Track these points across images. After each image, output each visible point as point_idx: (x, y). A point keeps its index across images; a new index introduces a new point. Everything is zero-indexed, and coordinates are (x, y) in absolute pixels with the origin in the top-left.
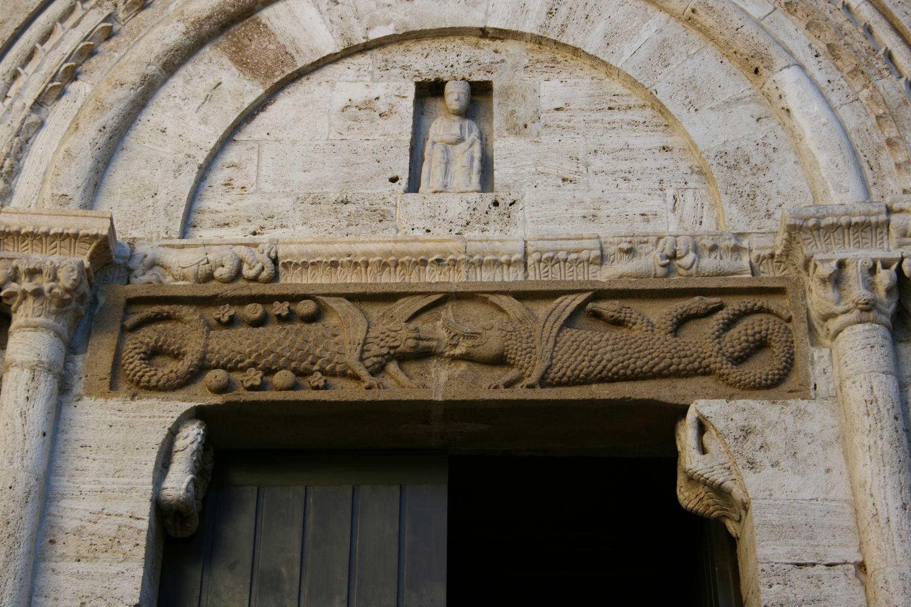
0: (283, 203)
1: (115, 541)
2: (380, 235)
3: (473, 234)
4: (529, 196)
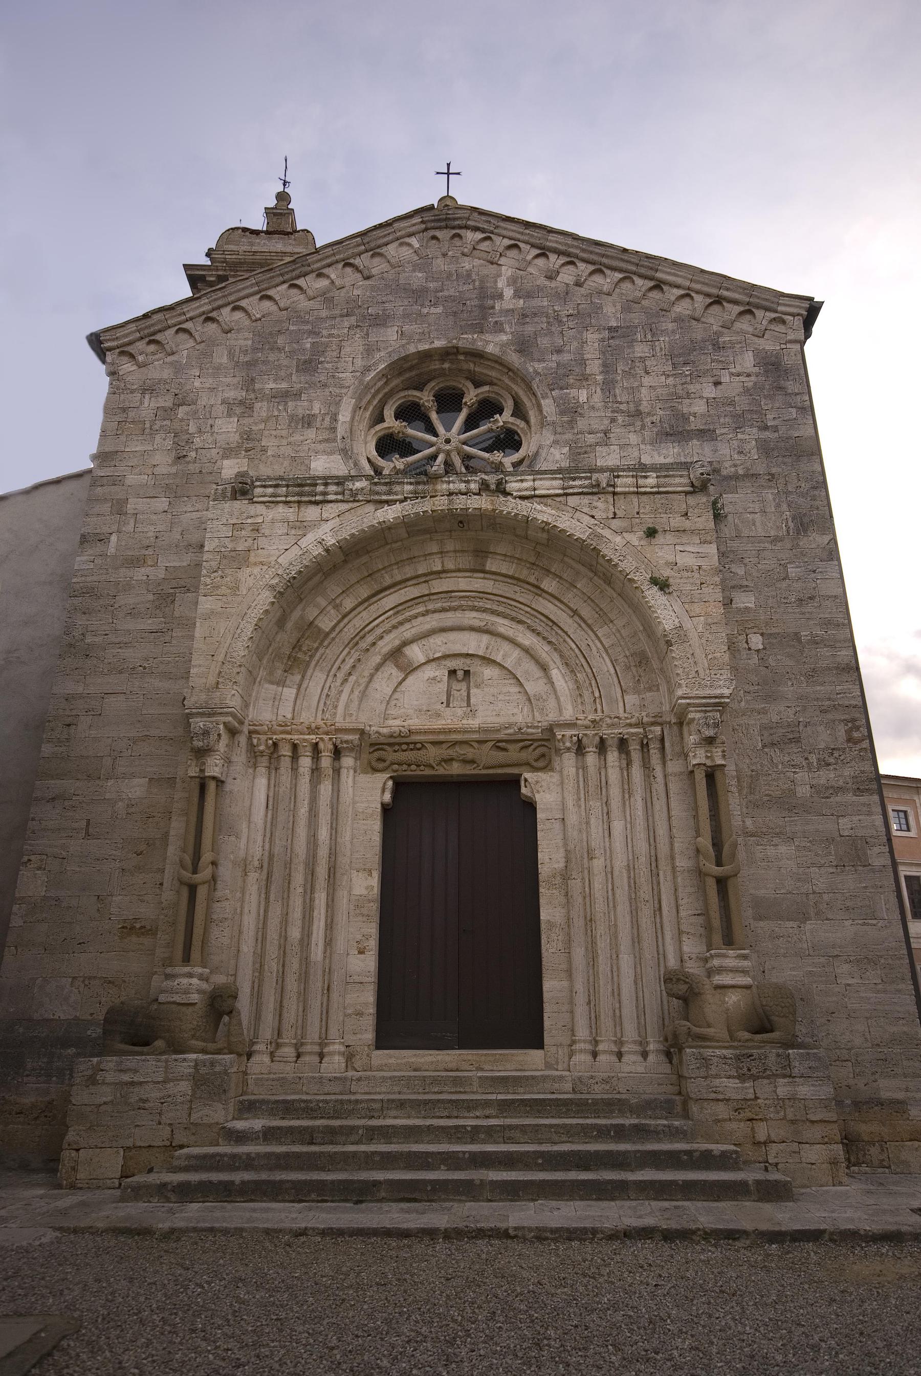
0: (411, 712)
1: (372, 815)
2: (439, 722)
3: (464, 722)
4: (481, 708)
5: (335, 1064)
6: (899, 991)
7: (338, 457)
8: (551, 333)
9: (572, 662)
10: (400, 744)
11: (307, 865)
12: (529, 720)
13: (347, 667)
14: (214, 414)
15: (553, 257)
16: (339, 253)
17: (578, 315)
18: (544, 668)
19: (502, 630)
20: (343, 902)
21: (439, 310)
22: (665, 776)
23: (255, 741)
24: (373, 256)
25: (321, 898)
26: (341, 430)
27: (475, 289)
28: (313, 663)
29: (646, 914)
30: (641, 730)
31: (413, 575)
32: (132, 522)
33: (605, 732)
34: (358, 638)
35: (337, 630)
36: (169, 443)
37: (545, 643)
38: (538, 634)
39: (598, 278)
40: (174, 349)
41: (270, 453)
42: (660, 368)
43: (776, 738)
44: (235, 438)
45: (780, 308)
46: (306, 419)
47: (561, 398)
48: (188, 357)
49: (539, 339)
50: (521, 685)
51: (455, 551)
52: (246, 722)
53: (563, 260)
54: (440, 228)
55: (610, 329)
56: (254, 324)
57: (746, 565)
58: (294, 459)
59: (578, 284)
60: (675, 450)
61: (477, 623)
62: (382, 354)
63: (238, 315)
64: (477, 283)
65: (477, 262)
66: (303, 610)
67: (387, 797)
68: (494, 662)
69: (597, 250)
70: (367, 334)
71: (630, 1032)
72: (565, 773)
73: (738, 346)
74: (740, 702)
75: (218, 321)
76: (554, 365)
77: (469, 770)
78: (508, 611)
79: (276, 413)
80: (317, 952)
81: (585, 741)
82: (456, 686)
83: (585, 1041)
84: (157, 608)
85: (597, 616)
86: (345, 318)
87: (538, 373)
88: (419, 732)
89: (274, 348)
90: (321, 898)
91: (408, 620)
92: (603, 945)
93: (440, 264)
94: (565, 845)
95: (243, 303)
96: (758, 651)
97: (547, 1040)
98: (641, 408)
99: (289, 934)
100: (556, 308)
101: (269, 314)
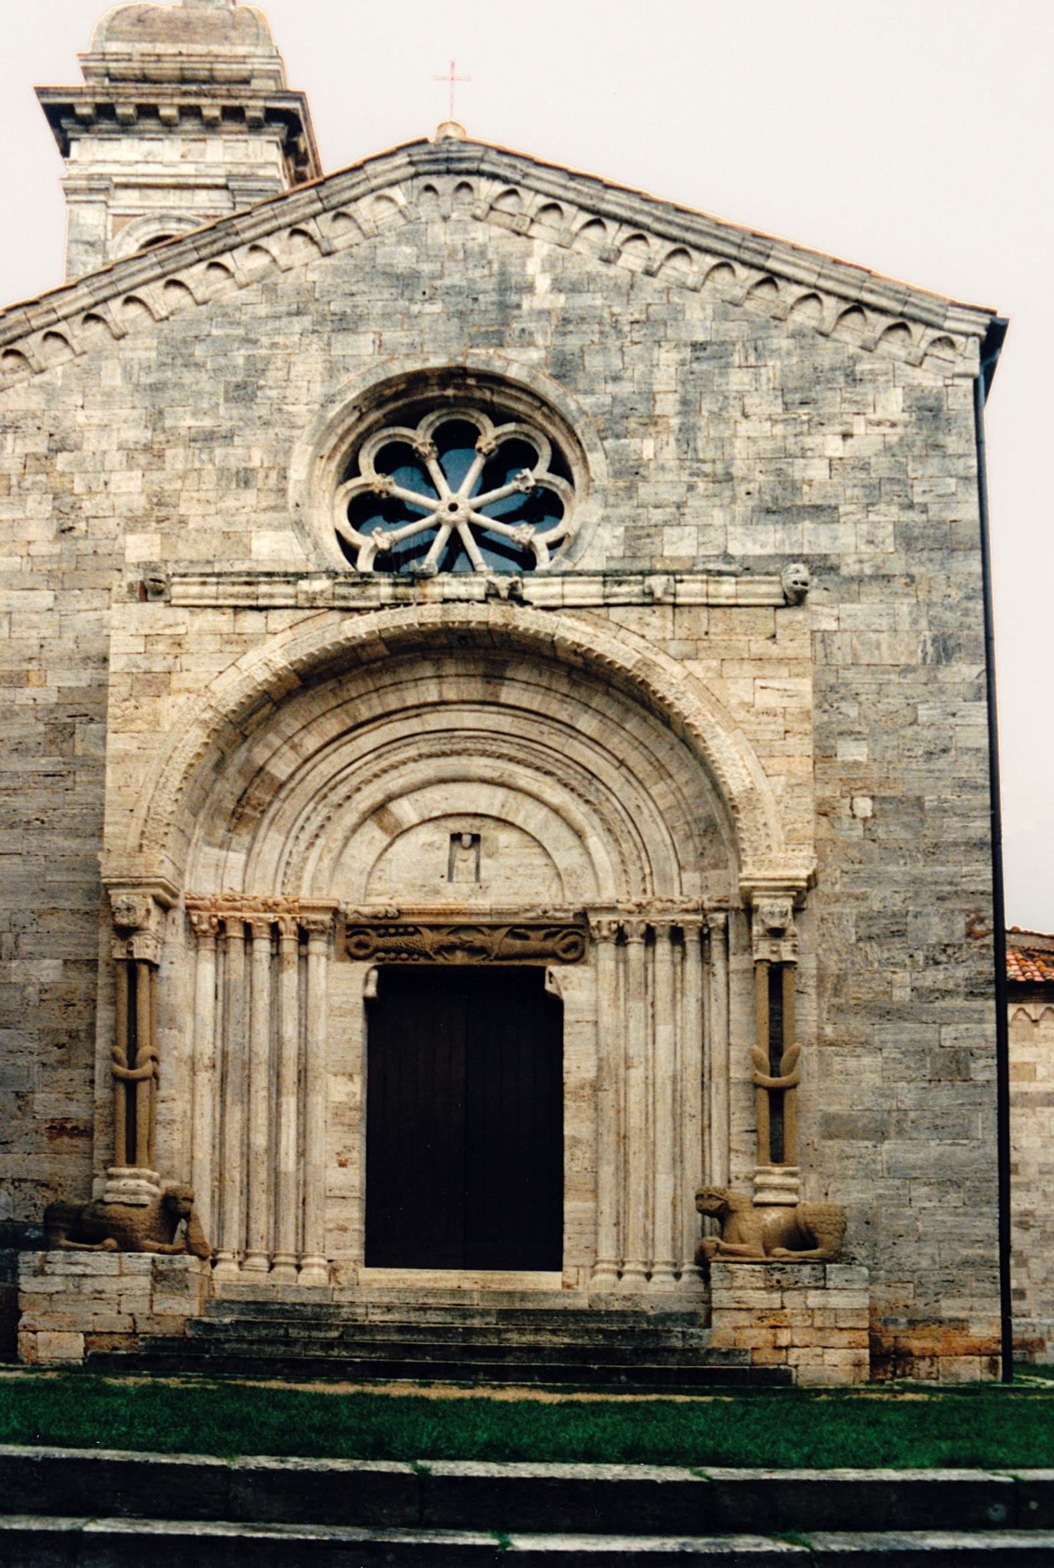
0: (401, 886)
1: (351, 1012)
3: (472, 901)
4: (494, 884)
5: (315, 1274)
6: (981, 1214)
7: (289, 534)
8: (605, 349)
9: (617, 829)
10: (387, 927)
11: (270, 1067)
12: (558, 901)
13: (311, 828)
14: (108, 466)
15: (612, 226)
16: (283, 214)
17: (648, 321)
18: (579, 835)
19: (522, 783)
20: (318, 1104)
21: (437, 308)
22: (728, 974)
23: (195, 919)
24: (336, 217)
25: (290, 1104)
26: (293, 495)
27: (491, 275)
28: (266, 822)
29: (691, 1130)
30: (700, 918)
31: (399, 706)
32: (5, 623)
33: (654, 918)
34: (325, 790)
35: (298, 777)
36: (47, 508)
37: (581, 801)
38: (572, 790)
39: (679, 262)
40: (44, 365)
41: (191, 526)
42: (766, 410)
43: (875, 930)
44: (141, 502)
45: (948, 324)
46: (242, 474)
47: (616, 452)
48: (65, 375)
49: (587, 358)
50: (548, 855)
51: (457, 675)
52: (182, 895)
53: (628, 231)
54: (438, 173)
55: (695, 346)
56: (159, 325)
57: (860, 703)
58: (227, 535)
59: (649, 273)
60: (778, 536)
61: (488, 774)
62: (352, 376)
63: (134, 310)
64: (496, 267)
65: (496, 231)
66: (250, 750)
67: (371, 990)
68: (512, 824)
69: (679, 219)
70: (329, 345)
71: (663, 1253)
72: (600, 967)
73: (882, 379)
74: (833, 884)
75: (104, 321)
76: (608, 400)
77: (476, 961)
78: (531, 759)
79: (197, 465)
80: (289, 1162)
81: (627, 929)
82: (460, 854)
83: (609, 1262)
84: (52, 742)
85: (650, 768)
86: (295, 319)
87: (585, 413)
88: (411, 913)
89: (192, 364)
90: (290, 1104)
91: (394, 767)
92: (637, 1164)
93: (439, 234)
94: (598, 1051)
95: (140, 293)
96: (865, 820)
97: (566, 1260)
98: (733, 470)
99: (252, 1140)
100: (616, 310)
101: (180, 310)
